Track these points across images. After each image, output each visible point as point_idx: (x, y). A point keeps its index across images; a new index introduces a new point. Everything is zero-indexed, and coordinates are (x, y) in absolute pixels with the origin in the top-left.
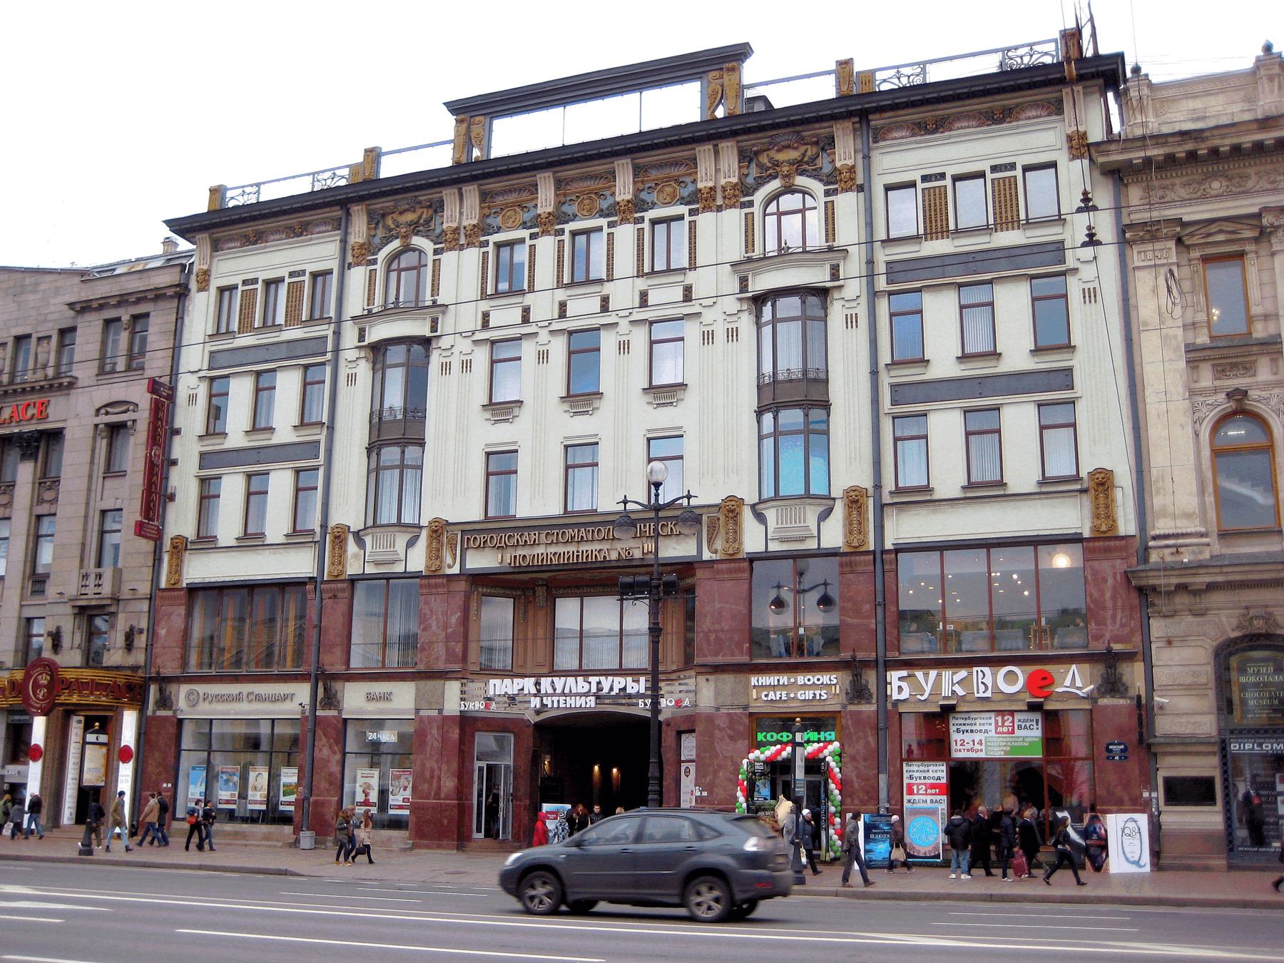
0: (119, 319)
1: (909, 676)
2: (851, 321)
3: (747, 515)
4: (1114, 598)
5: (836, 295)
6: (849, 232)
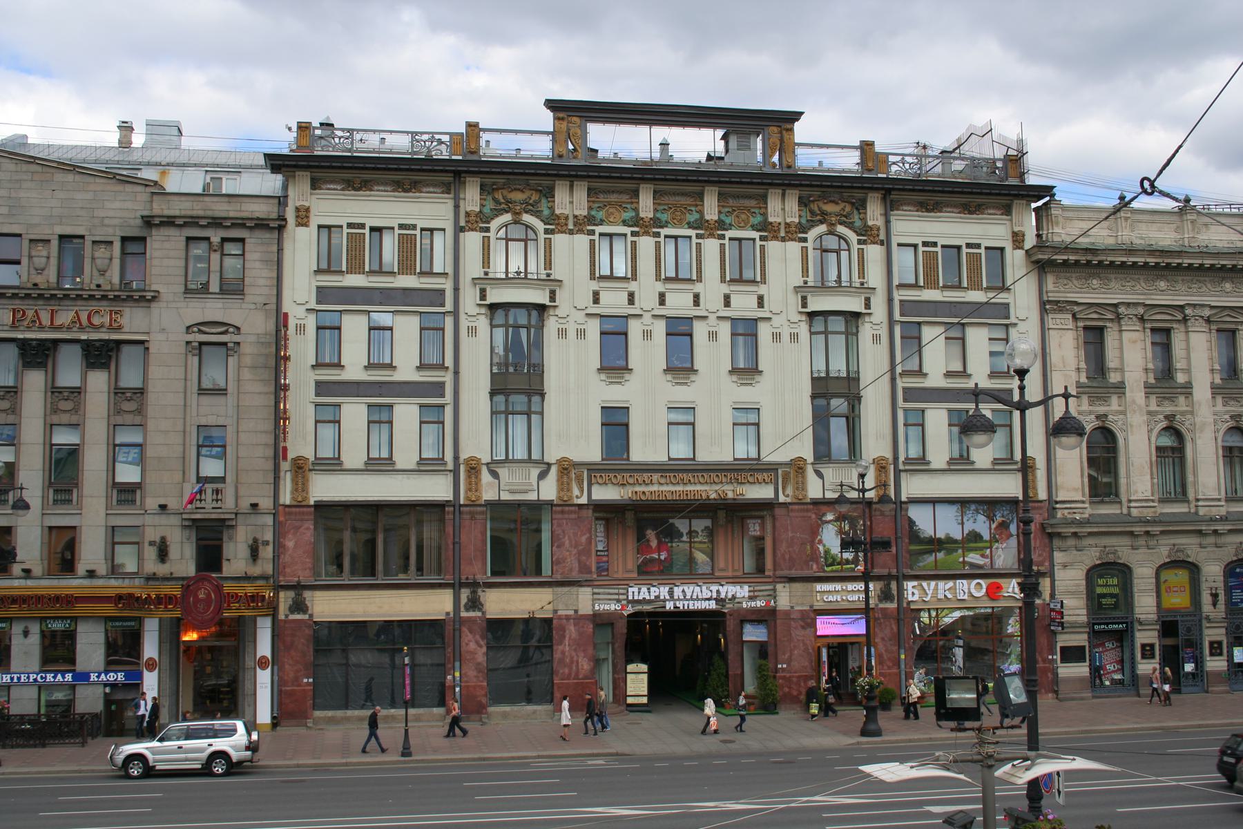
2: (876, 339)
5: (867, 319)
6: (875, 277)
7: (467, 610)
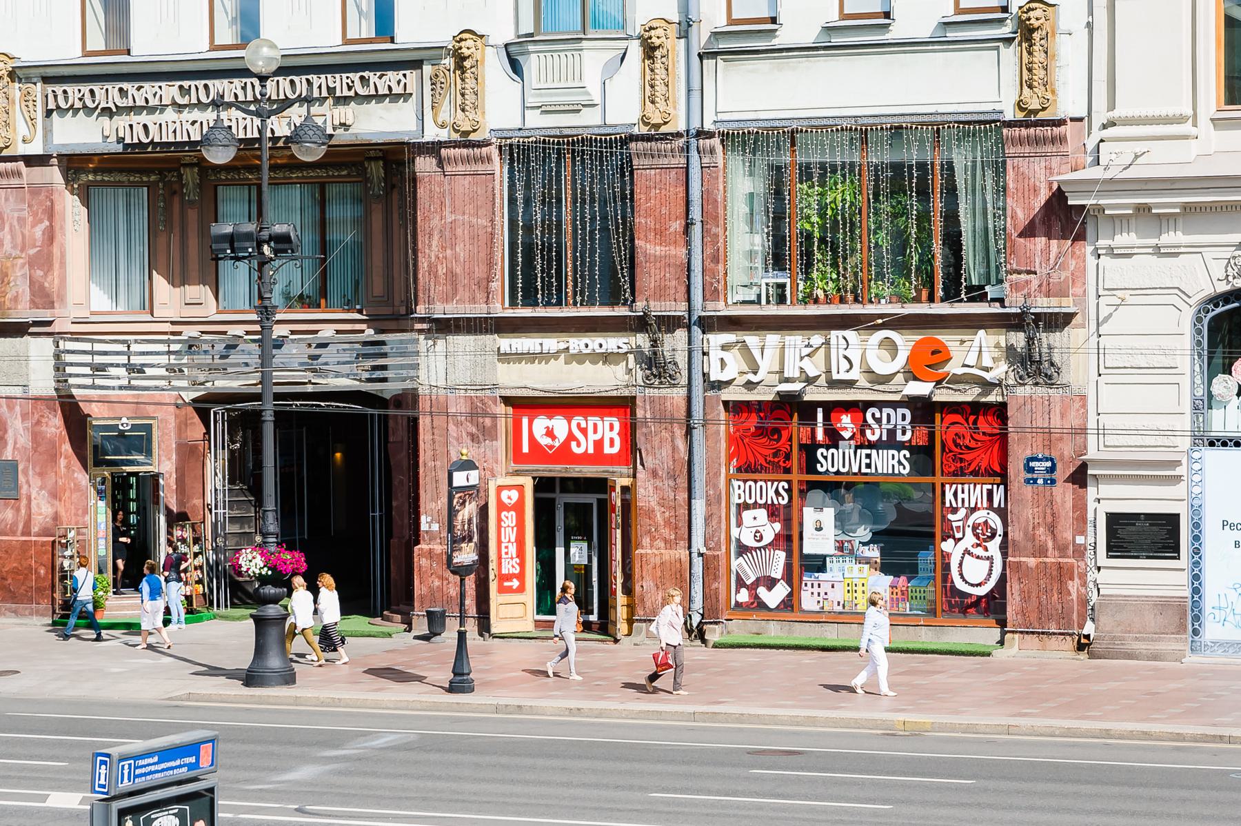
3: (494, 67)
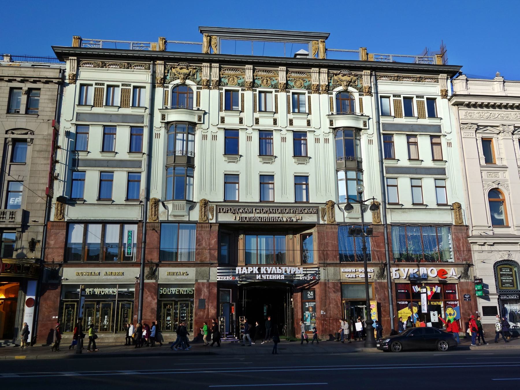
0: (21, 88)
1: (399, 270)
2: (370, 142)
4: (463, 246)
7: (148, 279)
